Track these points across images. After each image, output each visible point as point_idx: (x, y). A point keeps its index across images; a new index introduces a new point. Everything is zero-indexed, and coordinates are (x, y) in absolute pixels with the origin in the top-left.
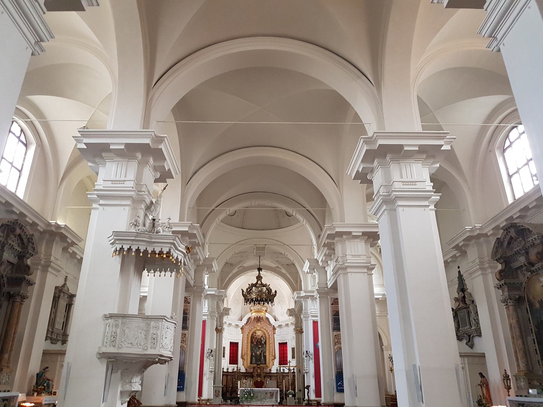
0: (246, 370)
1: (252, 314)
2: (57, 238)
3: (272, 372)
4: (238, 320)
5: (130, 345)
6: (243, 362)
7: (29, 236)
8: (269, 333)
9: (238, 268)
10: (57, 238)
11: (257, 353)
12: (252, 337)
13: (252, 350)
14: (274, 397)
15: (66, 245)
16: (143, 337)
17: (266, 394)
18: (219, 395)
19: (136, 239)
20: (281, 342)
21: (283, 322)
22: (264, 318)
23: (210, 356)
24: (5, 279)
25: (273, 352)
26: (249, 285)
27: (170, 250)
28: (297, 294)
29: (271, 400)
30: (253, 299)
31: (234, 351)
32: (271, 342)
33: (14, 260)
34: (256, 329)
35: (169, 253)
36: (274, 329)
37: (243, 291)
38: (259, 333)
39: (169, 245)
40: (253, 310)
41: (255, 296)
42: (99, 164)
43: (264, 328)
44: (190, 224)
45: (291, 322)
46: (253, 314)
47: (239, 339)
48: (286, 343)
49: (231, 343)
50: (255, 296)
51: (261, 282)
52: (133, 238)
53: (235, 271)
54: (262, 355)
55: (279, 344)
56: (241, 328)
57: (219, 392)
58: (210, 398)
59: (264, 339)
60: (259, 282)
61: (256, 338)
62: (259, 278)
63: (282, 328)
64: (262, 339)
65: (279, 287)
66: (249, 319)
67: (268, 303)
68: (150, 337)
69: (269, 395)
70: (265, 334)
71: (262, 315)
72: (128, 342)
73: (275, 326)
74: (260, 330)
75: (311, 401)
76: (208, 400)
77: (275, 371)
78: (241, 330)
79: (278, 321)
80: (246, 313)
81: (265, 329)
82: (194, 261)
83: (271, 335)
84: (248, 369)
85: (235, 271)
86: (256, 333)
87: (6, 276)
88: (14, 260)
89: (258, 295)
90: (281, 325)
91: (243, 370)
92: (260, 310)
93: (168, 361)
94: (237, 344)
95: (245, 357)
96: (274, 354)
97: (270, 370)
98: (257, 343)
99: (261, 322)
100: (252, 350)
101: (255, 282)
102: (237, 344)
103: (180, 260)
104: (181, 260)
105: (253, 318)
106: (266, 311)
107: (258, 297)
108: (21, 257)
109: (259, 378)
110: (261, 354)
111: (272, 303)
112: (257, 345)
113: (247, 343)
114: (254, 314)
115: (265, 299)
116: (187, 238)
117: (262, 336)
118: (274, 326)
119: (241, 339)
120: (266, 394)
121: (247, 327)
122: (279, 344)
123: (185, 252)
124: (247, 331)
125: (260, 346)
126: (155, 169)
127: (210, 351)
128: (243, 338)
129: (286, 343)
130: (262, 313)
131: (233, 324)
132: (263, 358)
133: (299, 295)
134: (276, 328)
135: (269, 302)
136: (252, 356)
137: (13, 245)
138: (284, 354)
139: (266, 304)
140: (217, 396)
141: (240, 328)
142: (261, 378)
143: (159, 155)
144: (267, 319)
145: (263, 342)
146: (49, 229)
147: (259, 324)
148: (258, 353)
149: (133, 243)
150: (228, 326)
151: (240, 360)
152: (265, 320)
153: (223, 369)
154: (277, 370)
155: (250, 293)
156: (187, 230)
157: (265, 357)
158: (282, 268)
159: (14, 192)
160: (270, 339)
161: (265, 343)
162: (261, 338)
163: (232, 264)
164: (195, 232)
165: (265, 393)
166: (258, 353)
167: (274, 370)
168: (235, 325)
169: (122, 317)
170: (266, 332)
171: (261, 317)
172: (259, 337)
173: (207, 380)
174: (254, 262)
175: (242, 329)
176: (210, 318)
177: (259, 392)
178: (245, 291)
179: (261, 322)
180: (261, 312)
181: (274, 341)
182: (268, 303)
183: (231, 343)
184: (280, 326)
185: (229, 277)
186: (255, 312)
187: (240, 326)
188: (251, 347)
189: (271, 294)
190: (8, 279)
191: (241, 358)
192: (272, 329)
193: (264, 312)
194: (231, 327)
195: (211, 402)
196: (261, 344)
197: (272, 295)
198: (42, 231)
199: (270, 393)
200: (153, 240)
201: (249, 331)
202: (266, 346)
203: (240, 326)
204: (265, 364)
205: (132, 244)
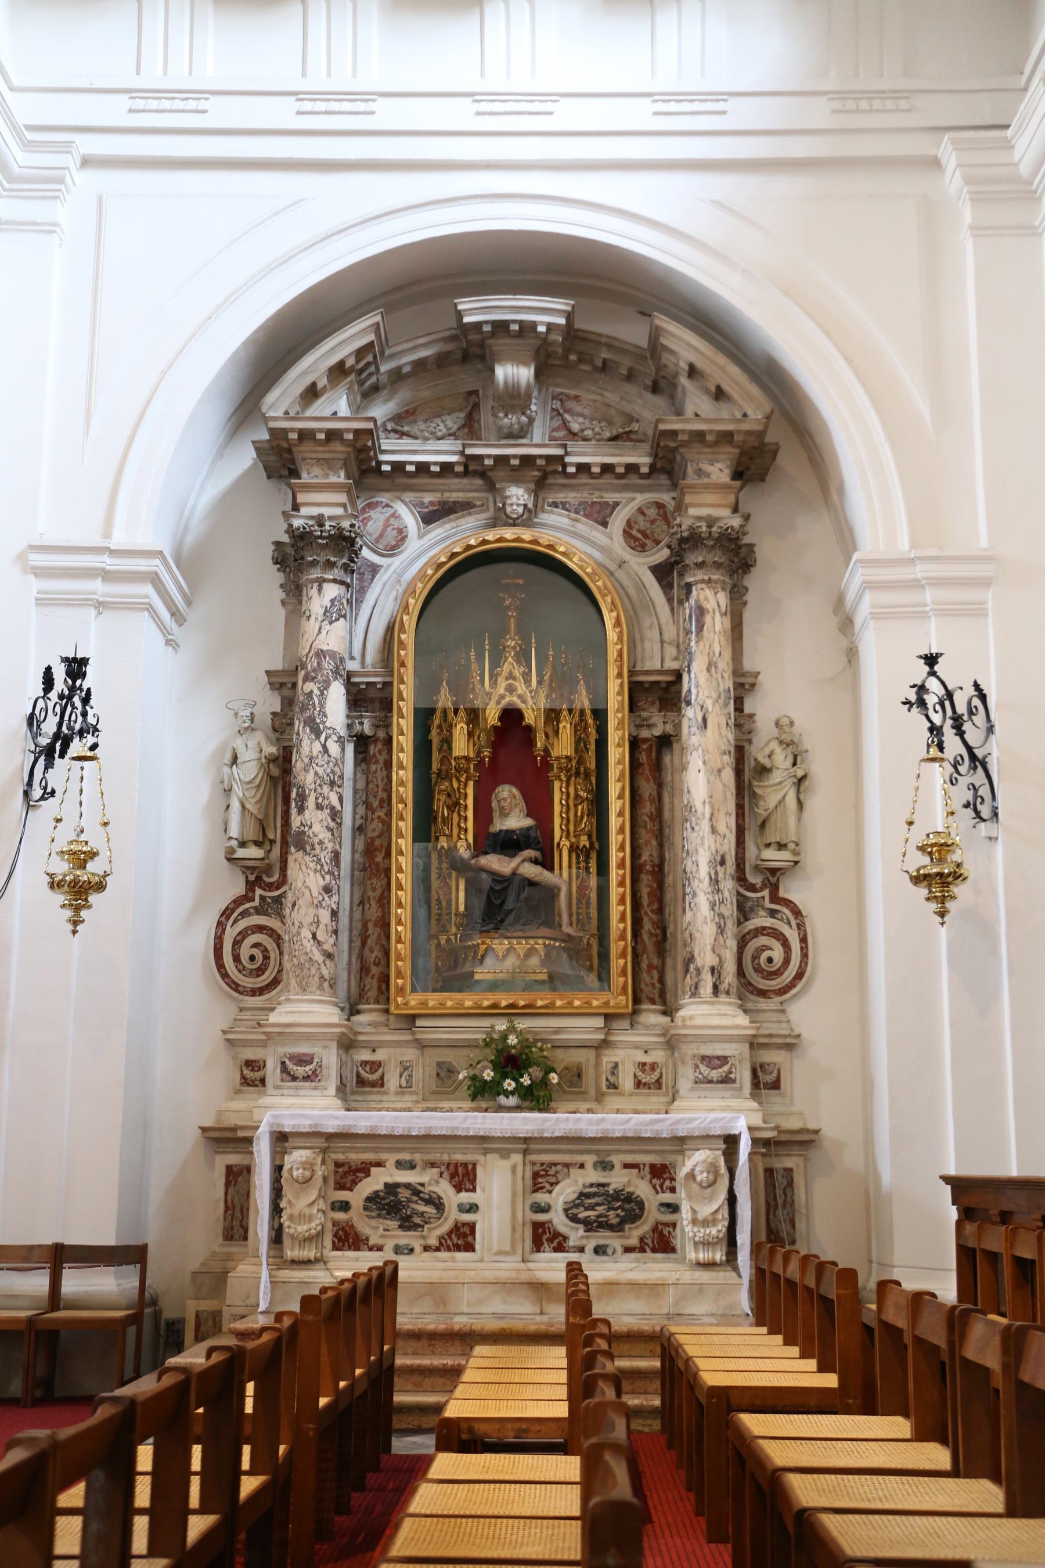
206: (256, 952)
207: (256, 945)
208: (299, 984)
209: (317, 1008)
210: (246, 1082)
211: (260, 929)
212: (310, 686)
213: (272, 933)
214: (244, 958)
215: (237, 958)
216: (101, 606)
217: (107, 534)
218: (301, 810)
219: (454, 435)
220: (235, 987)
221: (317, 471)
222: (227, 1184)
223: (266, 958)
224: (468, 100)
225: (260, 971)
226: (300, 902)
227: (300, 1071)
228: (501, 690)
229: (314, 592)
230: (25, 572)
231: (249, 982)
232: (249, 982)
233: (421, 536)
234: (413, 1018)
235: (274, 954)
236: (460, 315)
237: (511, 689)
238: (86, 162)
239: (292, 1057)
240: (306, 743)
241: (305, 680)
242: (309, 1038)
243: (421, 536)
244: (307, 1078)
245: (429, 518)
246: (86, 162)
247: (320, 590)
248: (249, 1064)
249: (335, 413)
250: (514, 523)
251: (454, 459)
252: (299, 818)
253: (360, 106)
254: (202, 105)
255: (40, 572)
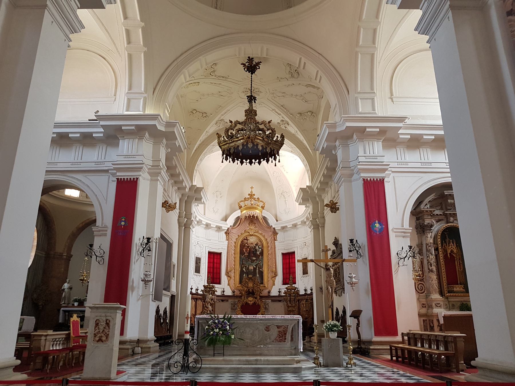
0: (234, 292)
1: (241, 212)
3: (273, 294)
4: (222, 220)
6: (228, 281)
8: (267, 240)
11: (250, 268)
12: (242, 246)
13: (243, 264)
14: (288, 336)
17: (267, 329)
18: (107, 336)
20: (285, 252)
21: (288, 222)
22: (260, 218)
23: (146, 252)
25: (274, 267)
26: (231, 122)
28: (328, 127)
29: (282, 345)
30: (238, 146)
31: (215, 264)
32: (270, 252)
34: (248, 234)
36: (275, 233)
38: (252, 240)
40: (243, 206)
43: (260, 232)
45: (302, 220)
46: (243, 213)
47: (222, 249)
48: (294, 253)
49: (210, 253)
54: (257, 271)
55: (283, 254)
56: (226, 233)
57: (108, 324)
58: (143, 337)
59: (260, 248)
61: (248, 246)
63: (287, 231)
64: (257, 248)
65: (283, 171)
66: (238, 218)
67: (268, 161)
69: (274, 332)
70: (261, 241)
71: (257, 212)
73: (276, 229)
74: (255, 235)
75: (364, 342)
76: (138, 341)
77: (277, 294)
78: (225, 235)
80: (233, 211)
81: (261, 234)
83: (270, 243)
84: (235, 290)
86: (247, 240)
89: (249, 138)
90: (287, 226)
91: (228, 292)
92: (254, 206)
94: (220, 254)
95: (232, 274)
96: (274, 269)
97: (269, 292)
98: (249, 253)
99: (255, 224)
100: (243, 264)
102: (220, 254)
105: (243, 217)
106: (263, 207)
107: (247, 143)
109: (250, 299)
110: (255, 269)
111: (275, 159)
112: (249, 257)
113: (234, 253)
114: (245, 211)
115: (262, 146)
117: (257, 244)
118: (274, 229)
119: (226, 248)
120: (267, 329)
121: (234, 231)
122: (283, 254)
124: (234, 237)
125: (254, 258)
127: (145, 241)
128: (228, 247)
129: (294, 253)
130: (257, 211)
131: (214, 225)
132: (258, 276)
133: (332, 130)
134: (276, 231)
135: (270, 158)
136: (242, 273)
138: (290, 268)
139: (264, 162)
140: (100, 340)
141: (224, 232)
142: (256, 298)
144: (264, 218)
145: (258, 253)
147: (252, 227)
148: (251, 268)
150: (205, 228)
151: (224, 278)
152: (261, 221)
153: (192, 289)
154: (279, 292)
157: (261, 274)
158: (290, 122)
160: (269, 248)
161: (262, 253)
162: (255, 247)
165: (262, 328)
166: (251, 268)
167: (274, 292)
168: (217, 226)
170: (263, 239)
171: (256, 216)
172: (252, 245)
173: (138, 300)
175: (227, 233)
176: (150, 178)
177: (248, 324)
179: (255, 224)
180: (256, 208)
181: (275, 251)
182: (268, 161)
183: (210, 253)
184: (283, 228)
186: (246, 209)
187: (223, 228)
188: (241, 260)
189: (273, 138)
191: (226, 275)
192: (271, 233)
193: (260, 208)
194: (210, 230)
195: (144, 346)
196: (255, 255)
197: (275, 141)
199: (278, 327)
201: (238, 237)
202: (262, 258)
203: (223, 228)
204: (262, 283)
206: (421, 287)
207: (421, 286)
208: (435, 292)
209: (437, 296)
210: (423, 307)
211: (421, 284)
212: (430, 248)
213: (422, 284)
214: (419, 288)
215: (418, 288)
216: (404, 237)
217: (403, 226)
218: (431, 266)
219: (439, 209)
220: (418, 292)
221: (426, 216)
222: (423, 322)
223: (422, 288)
224: (445, 163)
225: (422, 290)
226: (433, 280)
227: (439, 305)
228: (450, 247)
229: (428, 234)
230: (393, 232)
231: (420, 292)
232: (420, 292)
233: (436, 224)
234: (448, 297)
235: (423, 287)
236: (444, 193)
237: (452, 247)
238: (393, 172)
239: (437, 303)
240: (431, 256)
241: (429, 247)
242: (438, 301)
243: (436, 224)
244: (439, 306)
245: (437, 222)
246: (393, 172)
247: (429, 233)
248: (423, 304)
249: (428, 208)
250: (451, 223)
251: (442, 213)
252: (431, 268)
253: (430, 164)
254: (408, 164)
255: (395, 232)
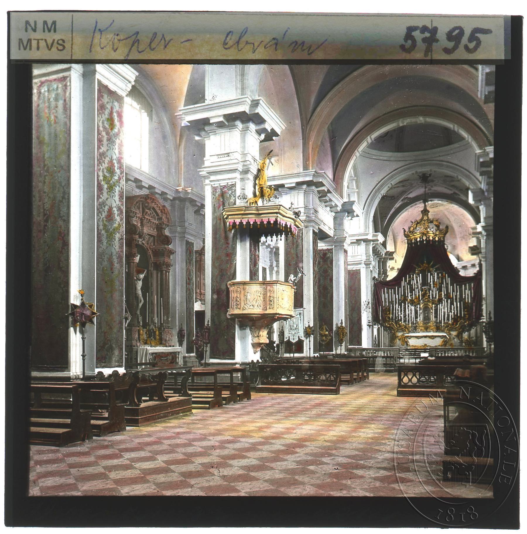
2: (188, 204)
5: (252, 307)
7: (161, 208)
9: (402, 201)
10: (188, 204)
15: (197, 208)
16: (262, 299)
19: (245, 212)
24: (150, 251)
27: (276, 219)
33: (154, 233)
35: (276, 221)
37: (405, 231)
39: (276, 215)
41: (420, 235)
42: (205, 138)
44: (313, 173)
50: (420, 235)
51: (428, 218)
52: (243, 212)
53: (397, 205)
60: (425, 218)
62: (425, 212)
68: (268, 299)
72: (250, 304)
79: (462, 260)
82: (331, 208)
85: (397, 205)
87: (150, 249)
88: (154, 233)
93: (288, 318)
101: (419, 218)
103: (289, 226)
104: (290, 226)
108: (160, 228)
115: (433, 237)
116: (314, 188)
123: (294, 217)
126: (259, 132)
137: (149, 219)
143: (258, 120)
146: (179, 195)
149: (243, 216)
155: (413, 233)
156: (311, 179)
159: (139, 168)
163: (393, 197)
164: (321, 180)
169: (243, 284)
174: (419, 191)
178: (407, 230)
185: (391, 213)
190: (152, 250)
198: (172, 199)
200: (260, 212)
205: (243, 218)
